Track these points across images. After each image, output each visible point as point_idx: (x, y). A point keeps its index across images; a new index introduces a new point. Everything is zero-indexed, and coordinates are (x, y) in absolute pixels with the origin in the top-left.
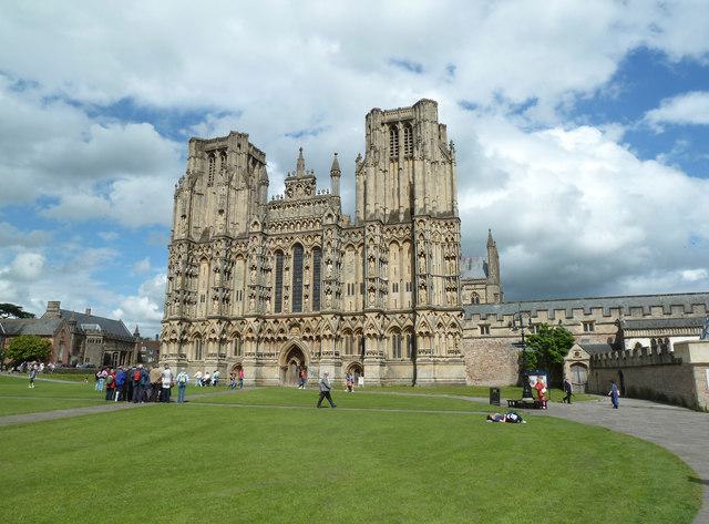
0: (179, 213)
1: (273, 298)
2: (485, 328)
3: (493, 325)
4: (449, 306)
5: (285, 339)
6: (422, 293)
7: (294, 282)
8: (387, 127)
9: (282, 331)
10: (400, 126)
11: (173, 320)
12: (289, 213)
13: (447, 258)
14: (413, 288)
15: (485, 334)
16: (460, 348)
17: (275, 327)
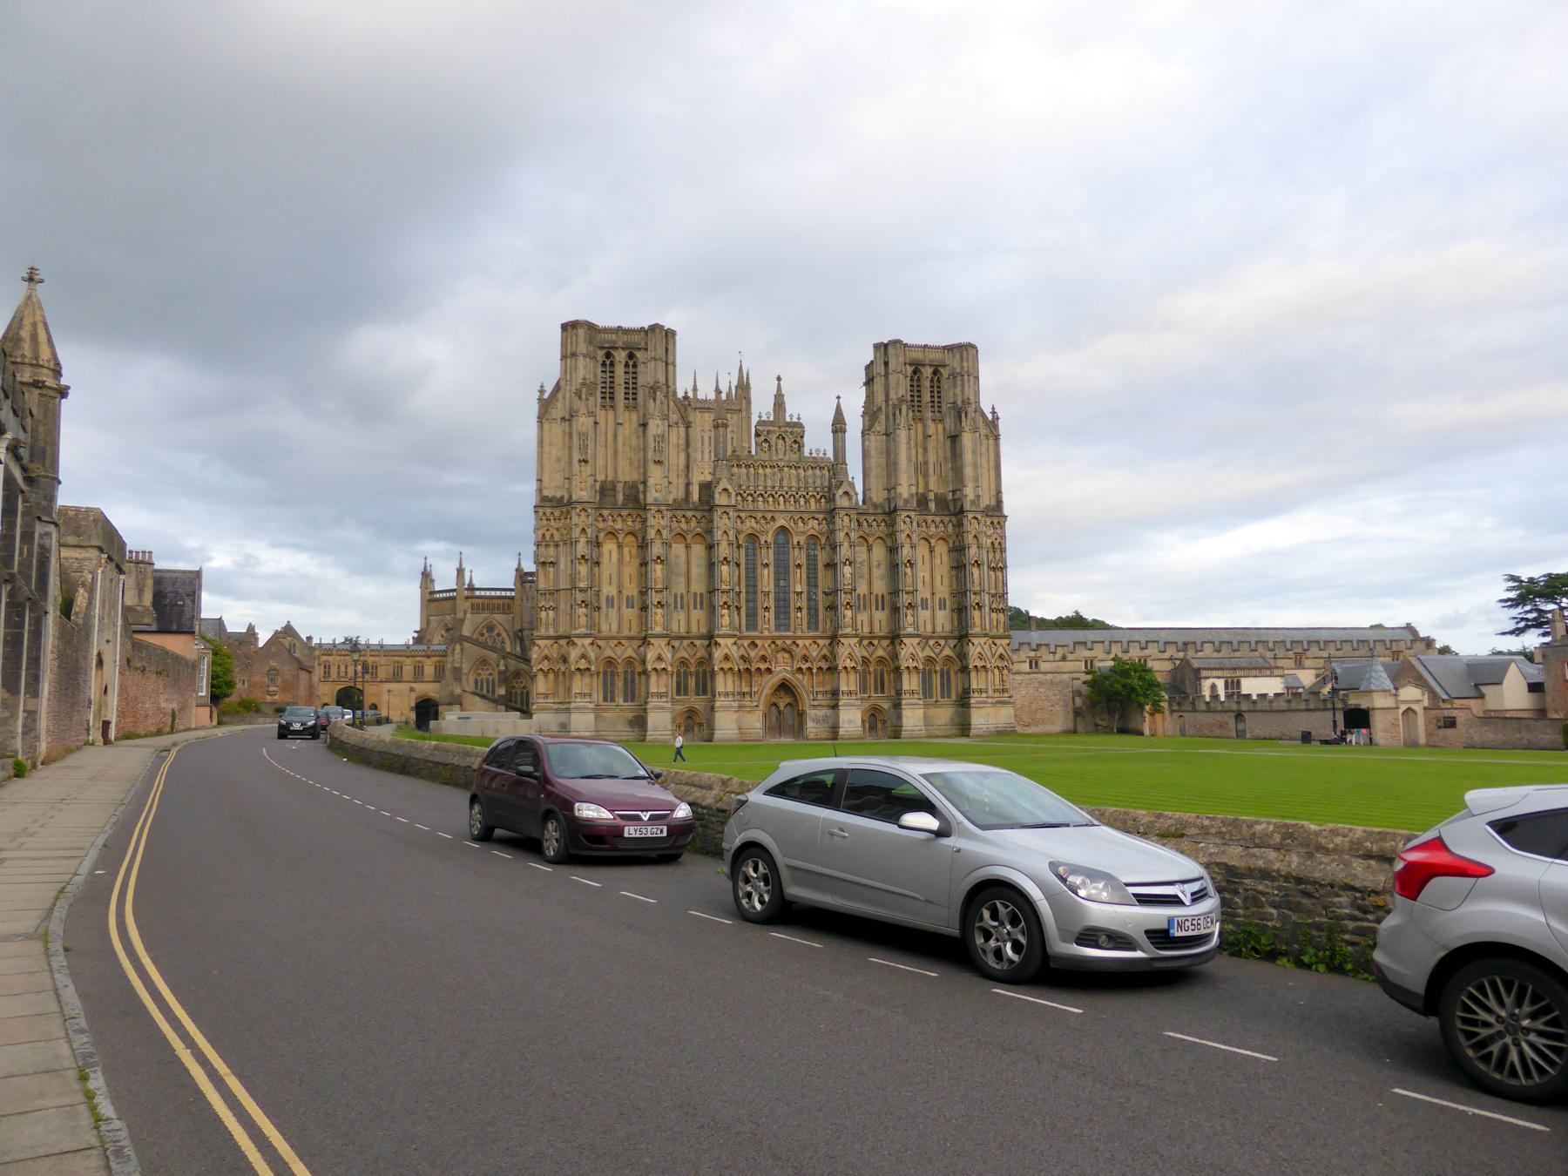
0: (576, 456)
1: (743, 611)
2: (1034, 663)
3: (1044, 658)
4: (994, 632)
5: (769, 670)
6: (976, 614)
7: (777, 585)
8: (910, 369)
9: (764, 659)
10: (927, 372)
11: (579, 636)
12: (769, 479)
13: (994, 569)
14: (961, 611)
15: (1034, 670)
16: (1007, 686)
17: (752, 654)
